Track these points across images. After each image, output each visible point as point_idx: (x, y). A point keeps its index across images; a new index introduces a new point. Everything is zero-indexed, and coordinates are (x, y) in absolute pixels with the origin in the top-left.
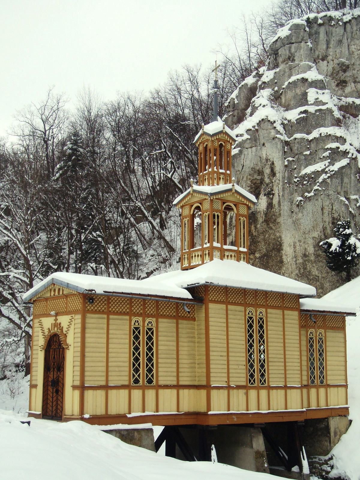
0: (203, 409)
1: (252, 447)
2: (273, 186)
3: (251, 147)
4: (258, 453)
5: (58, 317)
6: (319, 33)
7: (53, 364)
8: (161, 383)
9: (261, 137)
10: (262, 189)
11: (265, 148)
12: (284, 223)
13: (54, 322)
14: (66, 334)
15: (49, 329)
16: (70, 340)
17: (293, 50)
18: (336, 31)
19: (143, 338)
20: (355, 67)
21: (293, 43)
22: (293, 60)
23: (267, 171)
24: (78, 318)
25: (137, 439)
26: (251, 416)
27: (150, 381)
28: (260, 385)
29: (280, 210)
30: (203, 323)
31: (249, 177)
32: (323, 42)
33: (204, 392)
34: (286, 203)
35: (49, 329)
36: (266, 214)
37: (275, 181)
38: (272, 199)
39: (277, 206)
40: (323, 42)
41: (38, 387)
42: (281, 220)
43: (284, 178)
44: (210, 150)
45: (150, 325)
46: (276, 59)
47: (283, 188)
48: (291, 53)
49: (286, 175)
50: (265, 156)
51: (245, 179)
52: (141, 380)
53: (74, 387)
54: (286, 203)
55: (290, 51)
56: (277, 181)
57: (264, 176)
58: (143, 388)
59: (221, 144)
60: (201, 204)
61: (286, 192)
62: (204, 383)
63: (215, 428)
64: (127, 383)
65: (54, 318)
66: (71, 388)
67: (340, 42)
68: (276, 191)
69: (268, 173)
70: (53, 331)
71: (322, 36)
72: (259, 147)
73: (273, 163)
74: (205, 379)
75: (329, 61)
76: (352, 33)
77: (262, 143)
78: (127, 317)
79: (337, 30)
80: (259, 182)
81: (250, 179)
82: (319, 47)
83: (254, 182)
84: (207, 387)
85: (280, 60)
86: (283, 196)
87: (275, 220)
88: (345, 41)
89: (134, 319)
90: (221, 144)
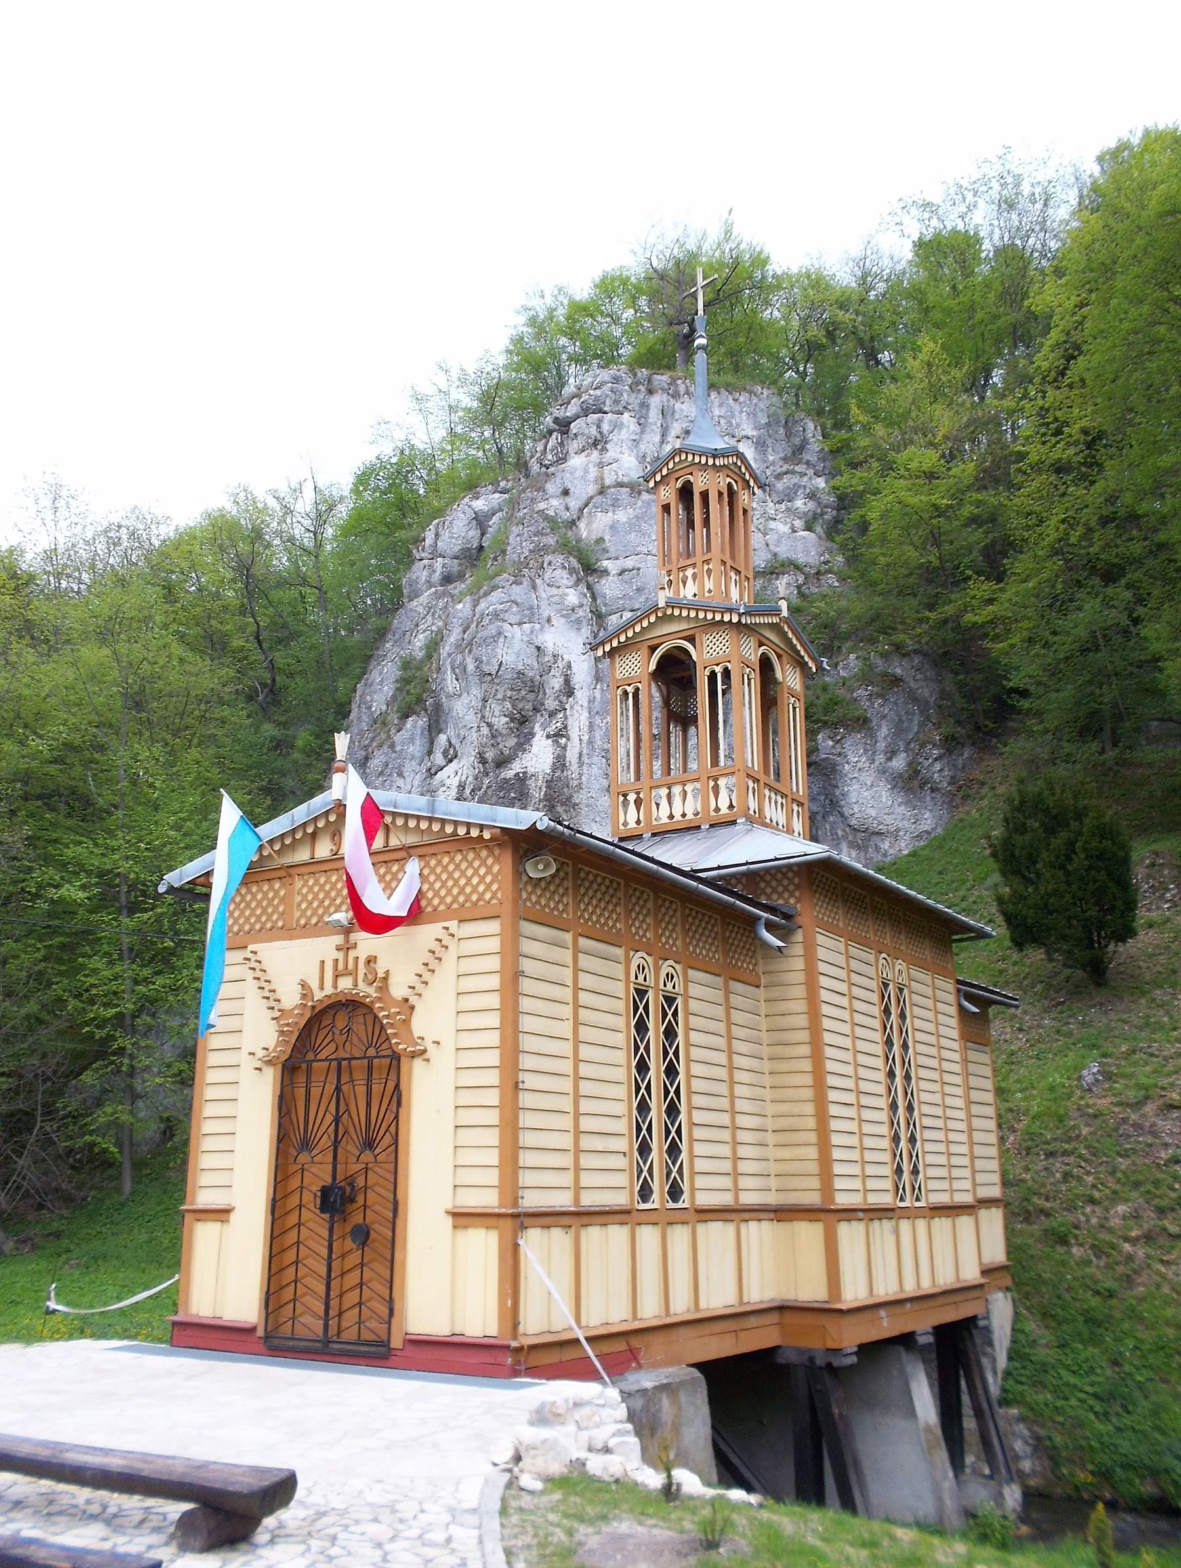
0: (812, 1291)
1: (911, 1413)
2: (566, 718)
3: (520, 624)
4: (928, 1429)
6: (648, 406)
7: (329, 1118)
8: (704, 1200)
9: (543, 604)
10: (537, 725)
12: (588, 806)
13: (340, 956)
14: (407, 1000)
15: (304, 985)
16: (433, 1022)
17: (605, 427)
18: (682, 410)
19: (655, 1033)
21: (606, 413)
22: (604, 449)
23: (556, 683)
24: (486, 937)
25: (670, 1422)
26: (908, 1305)
27: (675, 1192)
28: (918, 1204)
29: (581, 775)
30: (800, 992)
31: (509, 693)
32: (654, 427)
33: (809, 1233)
34: (596, 759)
35: (304, 985)
36: (549, 783)
37: (572, 707)
38: (564, 748)
39: (574, 767)
40: (654, 427)
41: (232, 1216)
42: (580, 798)
43: (591, 701)
44: (705, 495)
45: (669, 986)
46: (562, 444)
47: (591, 725)
48: (600, 433)
49: (598, 695)
51: (500, 696)
52: (655, 1186)
53: (462, 1218)
54: (596, 759)
55: (599, 427)
56: (577, 707)
57: (545, 694)
58: (665, 1221)
59: (729, 484)
60: (691, 639)
61: (598, 735)
62: (813, 1199)
63: (854, 1359)
64: (620, 1199)
65: (339, 939)
66: (449, 1220)
68: (574, 733)
69: (557, 687)
70: (329, 990)
71: (654, 415)
72: (537, 626)
73: (569, 666)
74: (815, 1183)
77: (546, 615)
78: (619, 952)
79: (683, 407)
80: (529, 706)
82: (647, 437)
83: (520, 706)
84: (827, 1214)
86: (591, 742)
87: (569, 798)
89: (637, 959)
90: (729, 484)
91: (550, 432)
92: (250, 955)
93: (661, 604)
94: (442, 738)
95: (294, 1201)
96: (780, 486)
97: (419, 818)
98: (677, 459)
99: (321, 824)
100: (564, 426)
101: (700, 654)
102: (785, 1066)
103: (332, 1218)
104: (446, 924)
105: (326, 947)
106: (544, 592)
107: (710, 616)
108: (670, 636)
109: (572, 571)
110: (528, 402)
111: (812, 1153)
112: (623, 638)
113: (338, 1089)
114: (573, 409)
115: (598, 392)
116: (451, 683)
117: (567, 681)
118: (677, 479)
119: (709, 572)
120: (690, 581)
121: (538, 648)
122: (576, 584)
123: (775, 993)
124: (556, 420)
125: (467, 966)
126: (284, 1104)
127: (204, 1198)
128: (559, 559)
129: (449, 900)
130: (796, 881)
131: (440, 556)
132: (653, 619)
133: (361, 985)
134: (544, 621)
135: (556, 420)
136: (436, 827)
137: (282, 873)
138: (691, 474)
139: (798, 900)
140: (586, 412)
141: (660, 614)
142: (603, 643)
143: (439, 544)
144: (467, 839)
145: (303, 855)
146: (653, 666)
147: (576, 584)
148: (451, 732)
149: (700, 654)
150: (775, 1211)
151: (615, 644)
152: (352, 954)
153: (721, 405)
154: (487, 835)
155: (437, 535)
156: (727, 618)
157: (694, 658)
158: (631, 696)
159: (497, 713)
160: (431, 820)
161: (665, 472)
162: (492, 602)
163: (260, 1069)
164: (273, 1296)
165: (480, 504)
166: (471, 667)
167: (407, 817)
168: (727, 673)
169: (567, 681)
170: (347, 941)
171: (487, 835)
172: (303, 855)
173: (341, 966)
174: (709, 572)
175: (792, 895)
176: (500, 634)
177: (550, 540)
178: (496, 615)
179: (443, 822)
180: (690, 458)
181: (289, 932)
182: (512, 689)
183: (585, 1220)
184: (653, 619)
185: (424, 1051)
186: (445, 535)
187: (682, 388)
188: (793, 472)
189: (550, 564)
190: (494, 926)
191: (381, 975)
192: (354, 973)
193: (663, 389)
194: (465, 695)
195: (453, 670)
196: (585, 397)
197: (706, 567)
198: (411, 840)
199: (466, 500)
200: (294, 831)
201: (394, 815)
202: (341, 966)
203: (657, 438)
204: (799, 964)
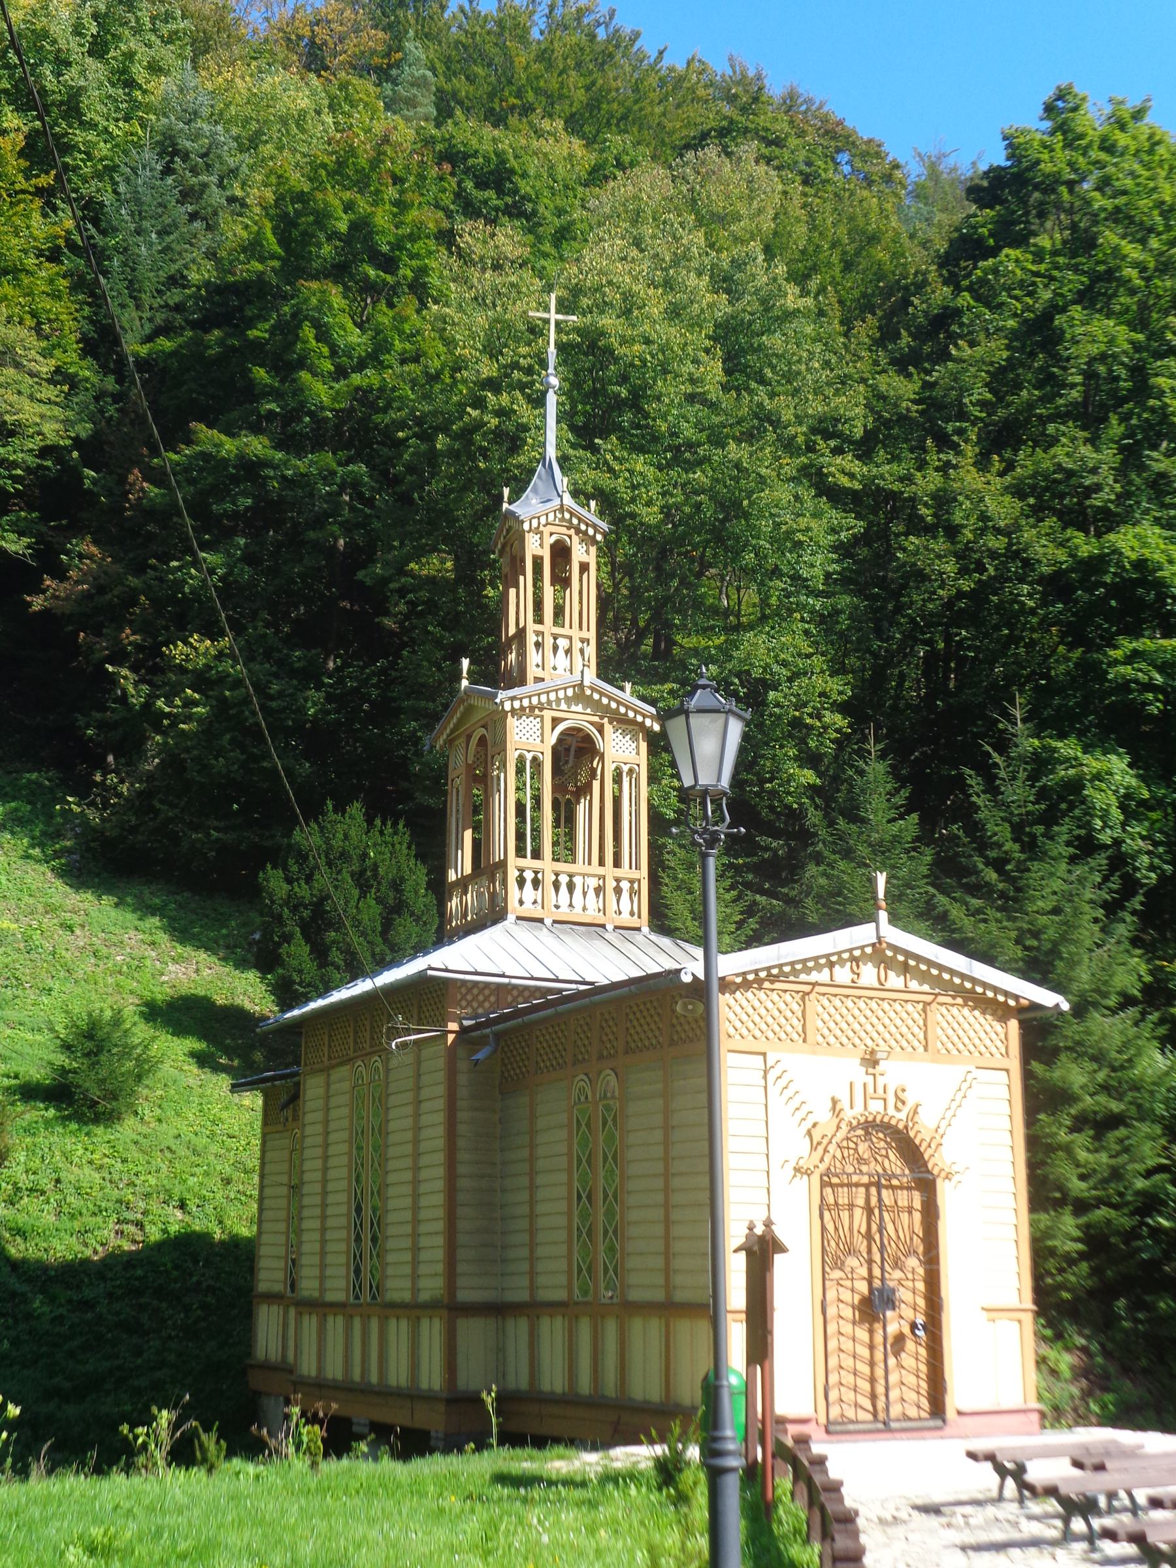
133: (891, 1111)
137: (807, 988)
146: (553, 740)
157: (600, 744)
171: (1012, 1003)
172: (823, 976)
173: (870, 1089)
191: (910, 1104)
202: (870, 1089)
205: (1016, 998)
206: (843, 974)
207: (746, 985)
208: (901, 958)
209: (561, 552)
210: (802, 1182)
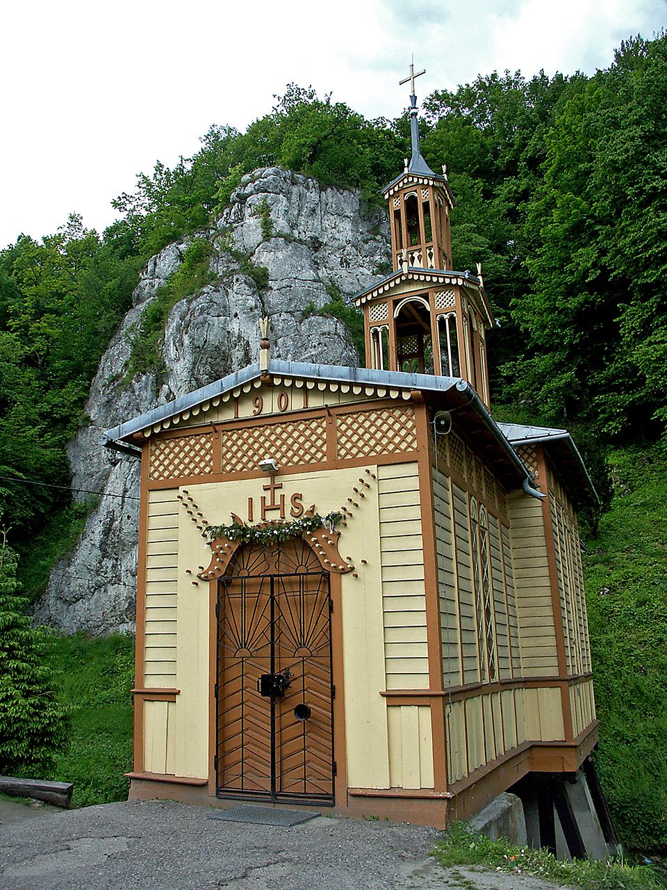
5: (278, 480)
11: (238, 321)
13: (268, 494)
17: (269, 201)
20: (326, 248)
21: (269, 192)
23: (238, 354)
33: (551, 696)
44: (426, 205)
46: (241, 210)
50: (237, 332)
53: (395, 699)
60: (426, 297)
67: (314, 210)
69: (240, 357)
70: (258, 520)
71: (294, 198)
73: (248, 345)
74: (554, 662)
75: (301, 231)
76: (327, 204)
77: (234, 313)
80: (221, 369)
81: (210, 363)
85: (247, 211)
88: (318, 211)
91: (234, 203)
92: (182, 494)
93: (405, 271)
94: (165, 387)
95: (236, 685)
96: (366, 247)
97: (340, 383)
98: (406, 181)
99: (247, 390)
100: (243, 199)
101: (432, 306)
102: (529, 583)
103: (273, 700)
104: (367, 468)
105: (256, 487)
106: (233, 297)
107: (441, 280)
108: (409, 293)
109: (250, 286)
110: (194, 198)
111: (552, 641)
112: (375, 294)
113: (272, 598)
114: (249, 189)
115: (265, 180)
116: (172, 353)
117: (247, 354)
118: (405, 194)
119: (431, 255)
120: (416, 260)
121: (229, 332)
122: (254, 293)
123: (520, 533)
124: (238, 195)
125: (386, 501)
126: (220, 612)
127: (151, 684)
128: (242, 277)
129: (366, 449)
130: (534, 455)
131: (157, 277)
132: (398, 281)
134: (232, 316)
135: (238, 195)
136: (357, 391)
137: (211, 429)
138: (416, 191)
139: (536, 469)
140: (258, 191)
141: (403, 278)
142: (360, 297)
143: (156, 270)
144: (388, 398)
145: (229, 416)
146: (396, 314)
147: (254, 293)
148: (171, 383)
149: (432, 306)
150: (524, 682)
151: (369, 298)
152: (278, 493)
153: (333, 196)
154: (406, 396)
155: (155, 264)
156: (454, 281)
158: (380, 333)
159: (201, 372)
160: (351, 385)
161: (396, 189)
162: (202, 301)
163: (197, 584)
164: (219, 761)
165: (182, 247)
166: (187, 341)
167: (328, 383)
168: (452, 319)
169: (247, 354)
170: (273, 481)
172: (229, 416)
173: (268, 503)
174: (431, 255)
175: (531, 465)
176: (206, 322)
177: (235, 266)
178: (202, 310)
179: (364, 386)
180: (416, 180)
181: (218, 476)
182: (211, 358)
183: (467, 695)
184: (398, 281)
185: (353, 569)
186: (161, 264)
187: (311, 184)
188: (375, 239)
189: (237, 280)
190: (413, 469)
191: (307, 508)
192: (281, 508)
193: (301, 183)
194: (182, 359)
195: (174, 343)
196: (257, 182)
197: (428, 251)
198: (331, 402)
199: (175, 244)
200: (221, 397)
201: (316, 381)
202: (268, 503)
203: (296, 212)
204: (539, 512)
205: (408, 390)
206: (247, 411)
207: (163, 436)
208: (299, 384)
209: (411, 203)
210: (205, 587)
